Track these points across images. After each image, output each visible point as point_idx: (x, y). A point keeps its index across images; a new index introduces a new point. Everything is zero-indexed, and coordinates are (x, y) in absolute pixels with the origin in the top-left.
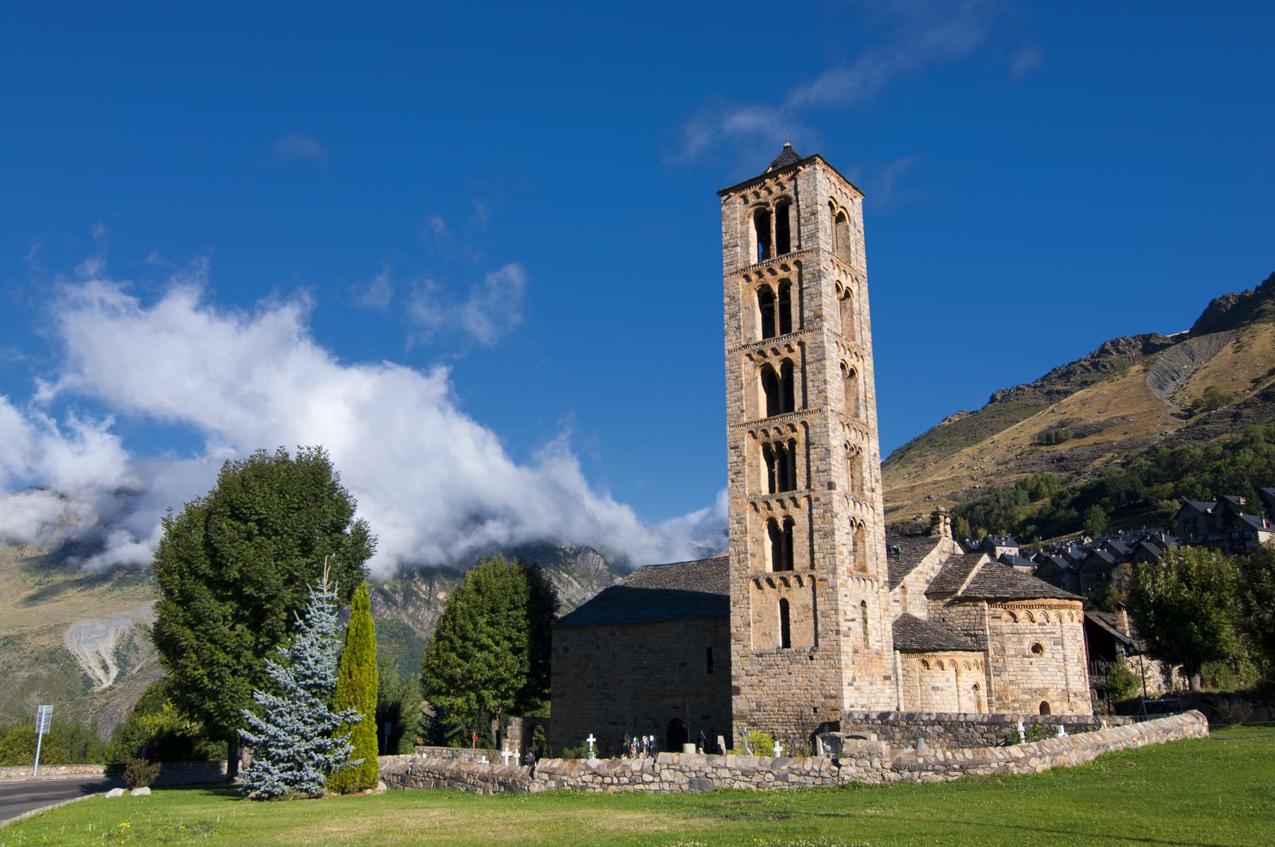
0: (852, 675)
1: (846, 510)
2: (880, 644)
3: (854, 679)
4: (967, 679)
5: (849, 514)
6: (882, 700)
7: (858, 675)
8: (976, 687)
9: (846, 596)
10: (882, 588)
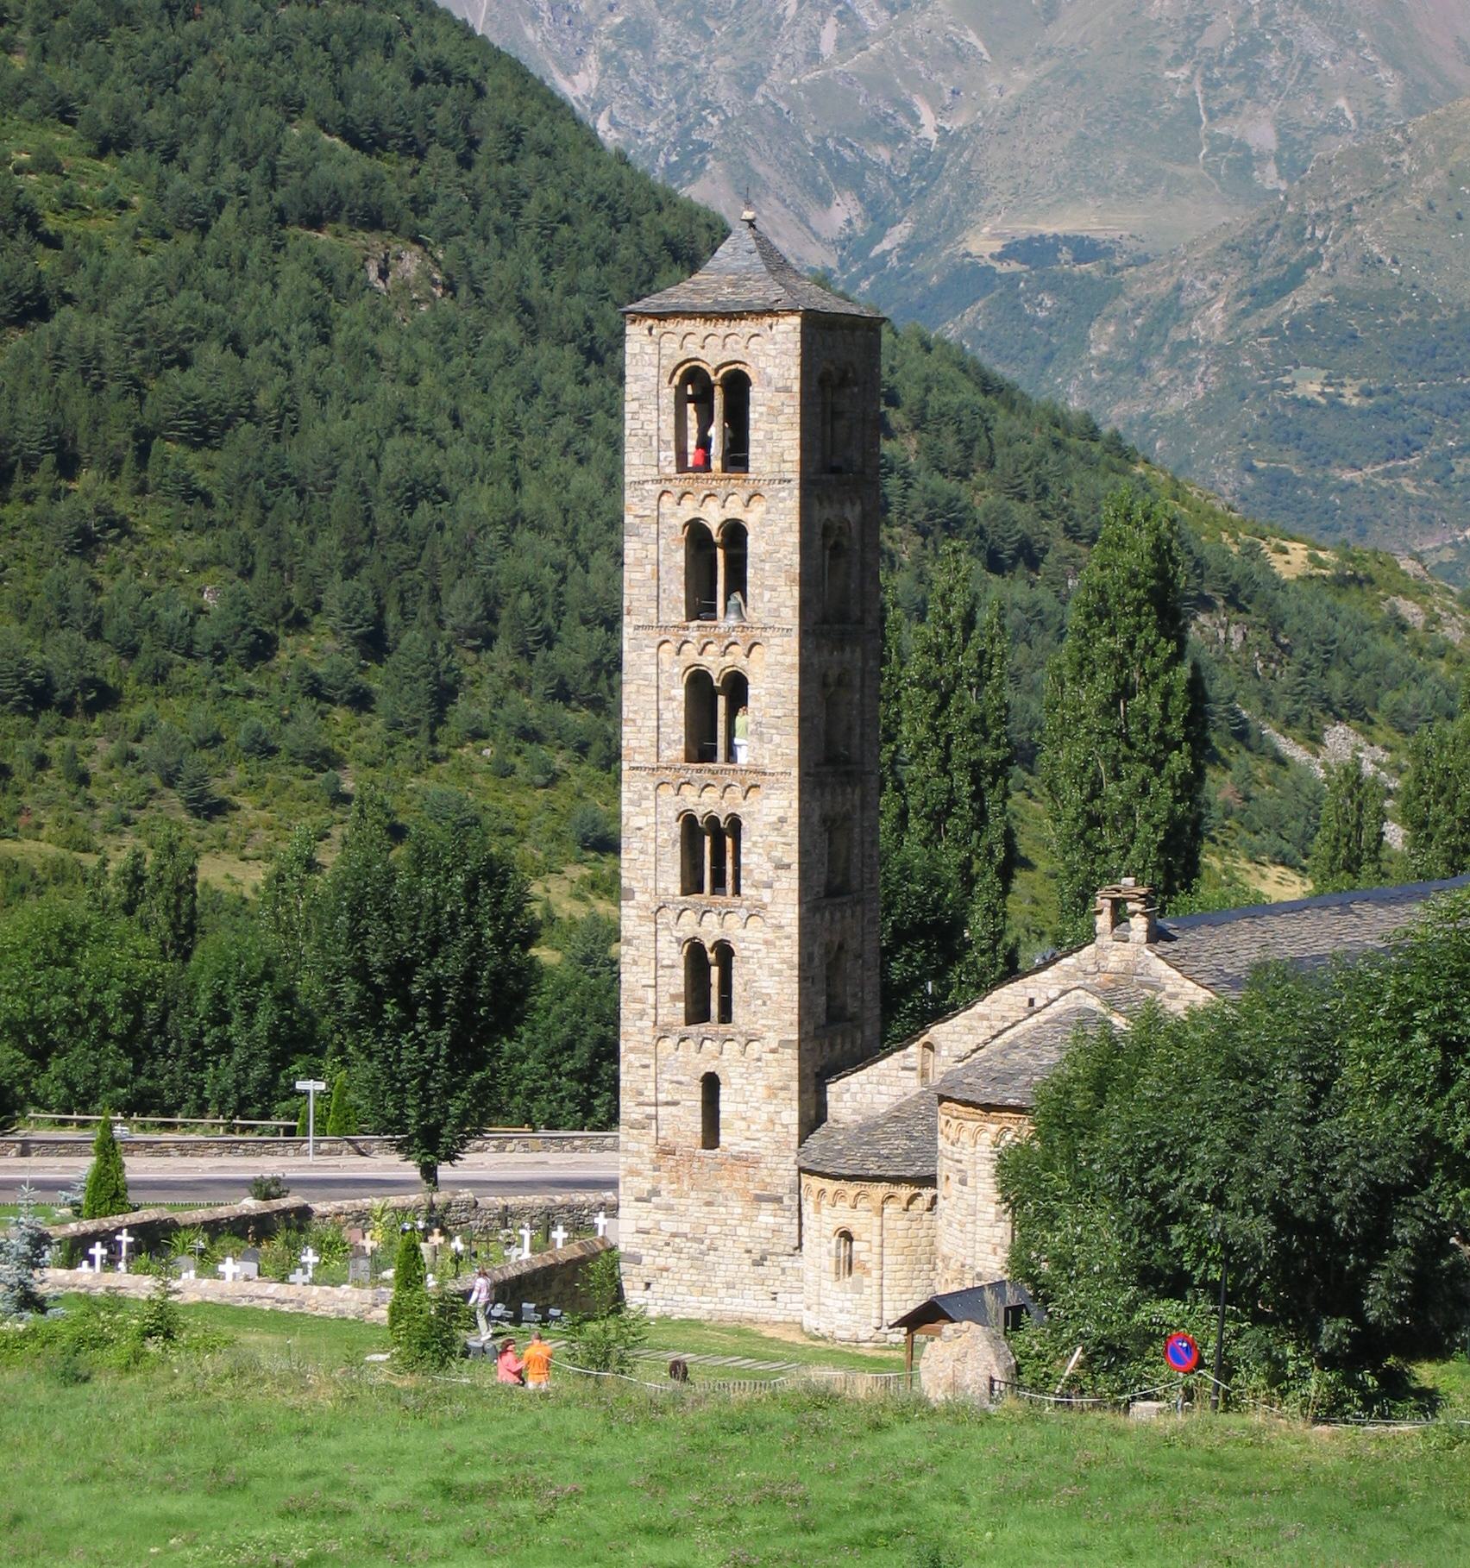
0: (649, 1187)
1: (668, 928)
2: (756, 1144)
3: (655, 1192)
4: (829, 1220)
5: (680, 935)
6: (740, 1231)
7: (664, 1186)
8: (847, 1236)
9: (646, 1066)
10: (773, 1051)
